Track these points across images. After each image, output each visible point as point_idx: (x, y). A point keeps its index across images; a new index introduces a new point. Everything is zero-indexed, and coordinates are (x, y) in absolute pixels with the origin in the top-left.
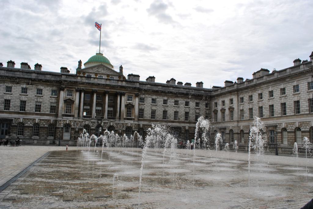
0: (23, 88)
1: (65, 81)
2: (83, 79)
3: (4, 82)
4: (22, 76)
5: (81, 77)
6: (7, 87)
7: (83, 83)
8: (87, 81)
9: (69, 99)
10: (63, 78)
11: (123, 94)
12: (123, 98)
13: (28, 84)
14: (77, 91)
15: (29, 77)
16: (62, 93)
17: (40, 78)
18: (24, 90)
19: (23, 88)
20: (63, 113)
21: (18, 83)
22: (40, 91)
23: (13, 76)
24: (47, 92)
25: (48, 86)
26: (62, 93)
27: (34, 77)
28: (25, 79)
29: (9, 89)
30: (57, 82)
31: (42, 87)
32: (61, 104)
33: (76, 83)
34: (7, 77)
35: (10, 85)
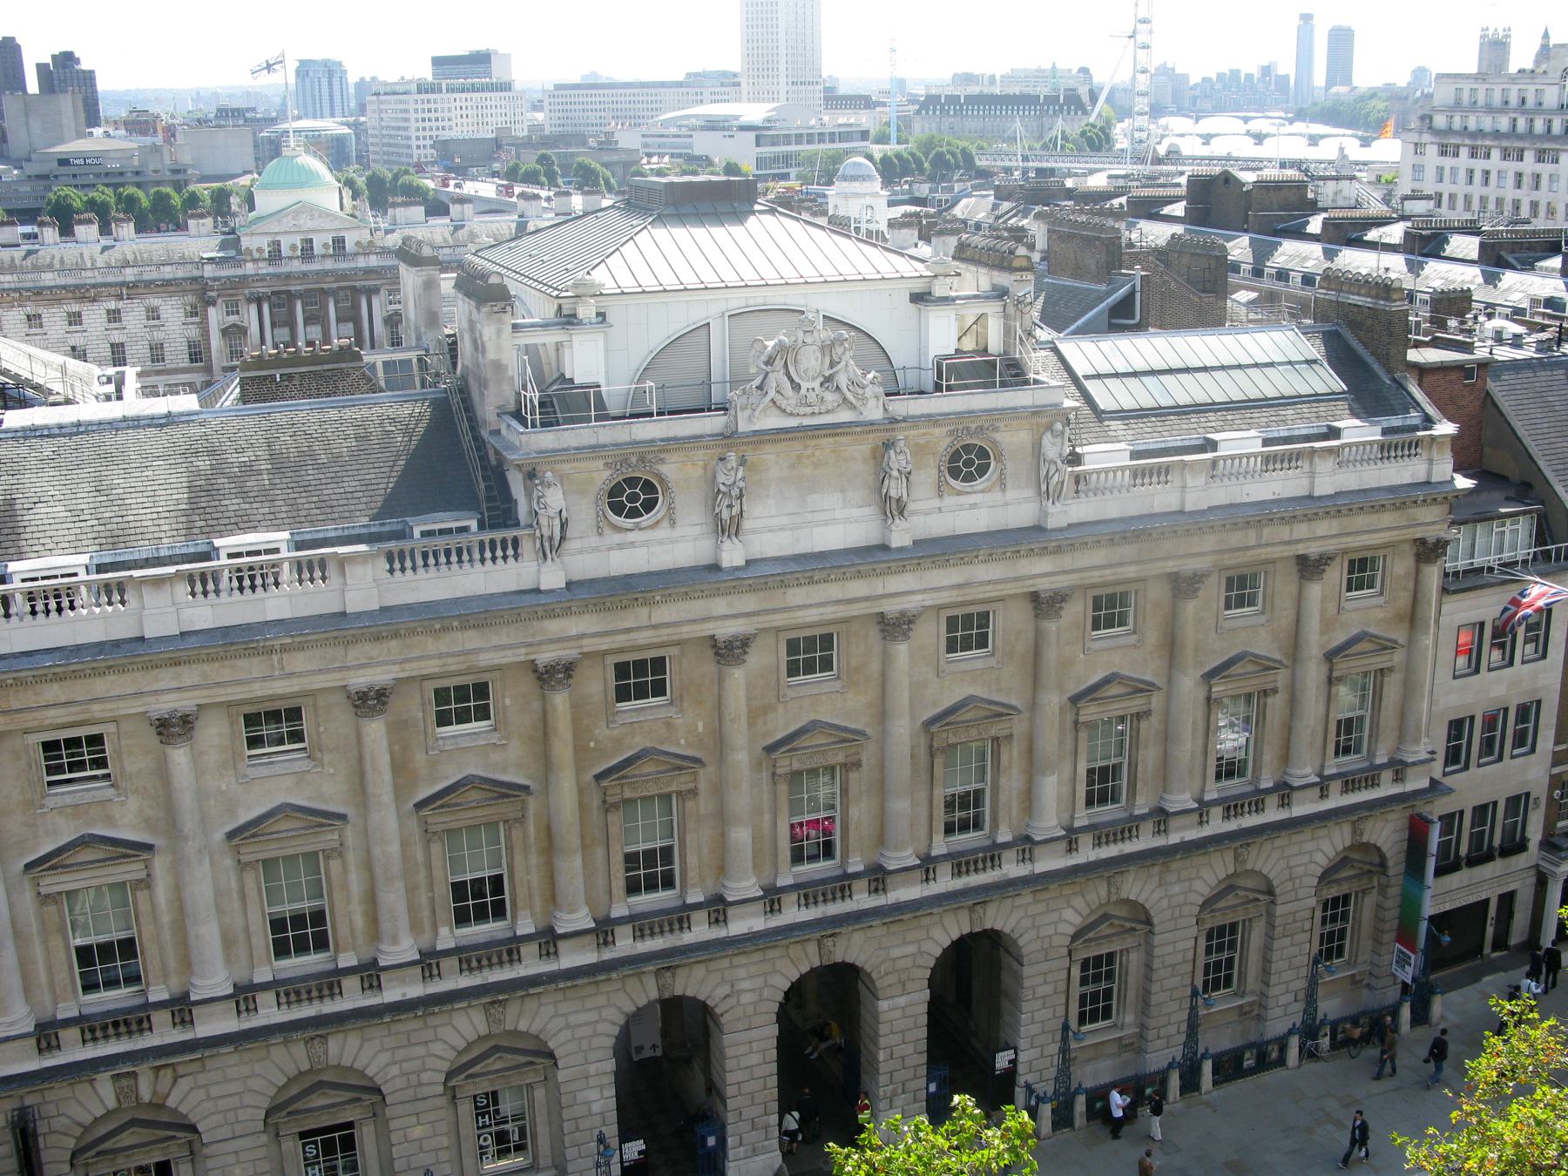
0: (108, 312)
1: (215, 279)
2: (261, 264)
3: (59, 301)
4: (100, 280)
5: (254, 261)
6: (69, 314)
7: (262, 278)
8: (271, 270)
9: (234, 325)
10: (209, 271)
11: (376, 290)
12: (376, 302)
13: (120, 297)
14: (249, 301)
15: (120, 279)
16: (212, 311)
17: (146, 277)
18: (114, 316)
19: (108, 312)
20: (225, 364)
21: (94, 300)
22: (153, 314)
23: (78, 282)
24: (173, 311)
25: (172, 294)
26: (212, 311)
27: (132, 278)
28: (110, 285)
29: (75, 319)
30: (194, 279)
31: (155, 302)
32: (216, 341)
33: (245, 277)
34: (64, 287)
35: (75, 308)
